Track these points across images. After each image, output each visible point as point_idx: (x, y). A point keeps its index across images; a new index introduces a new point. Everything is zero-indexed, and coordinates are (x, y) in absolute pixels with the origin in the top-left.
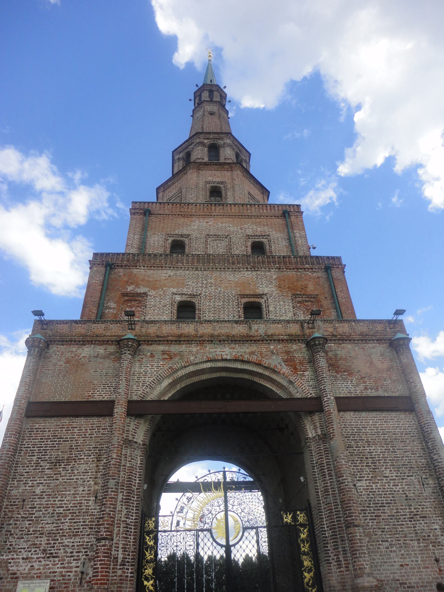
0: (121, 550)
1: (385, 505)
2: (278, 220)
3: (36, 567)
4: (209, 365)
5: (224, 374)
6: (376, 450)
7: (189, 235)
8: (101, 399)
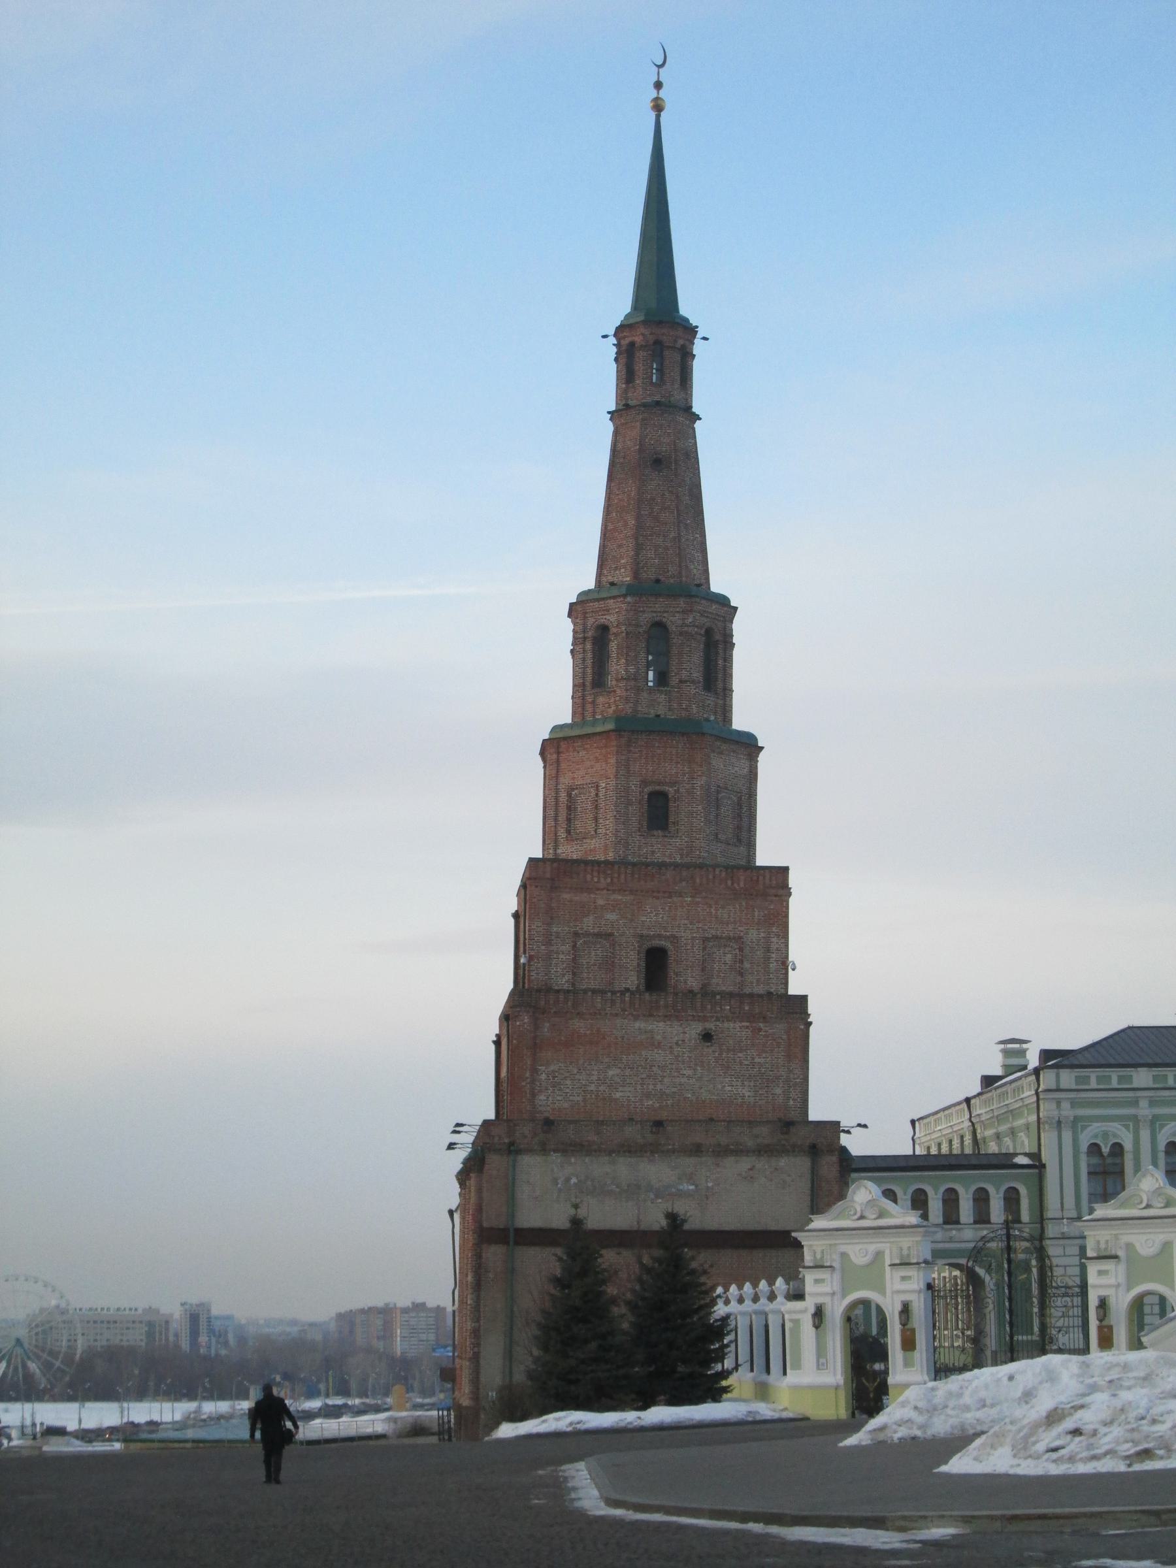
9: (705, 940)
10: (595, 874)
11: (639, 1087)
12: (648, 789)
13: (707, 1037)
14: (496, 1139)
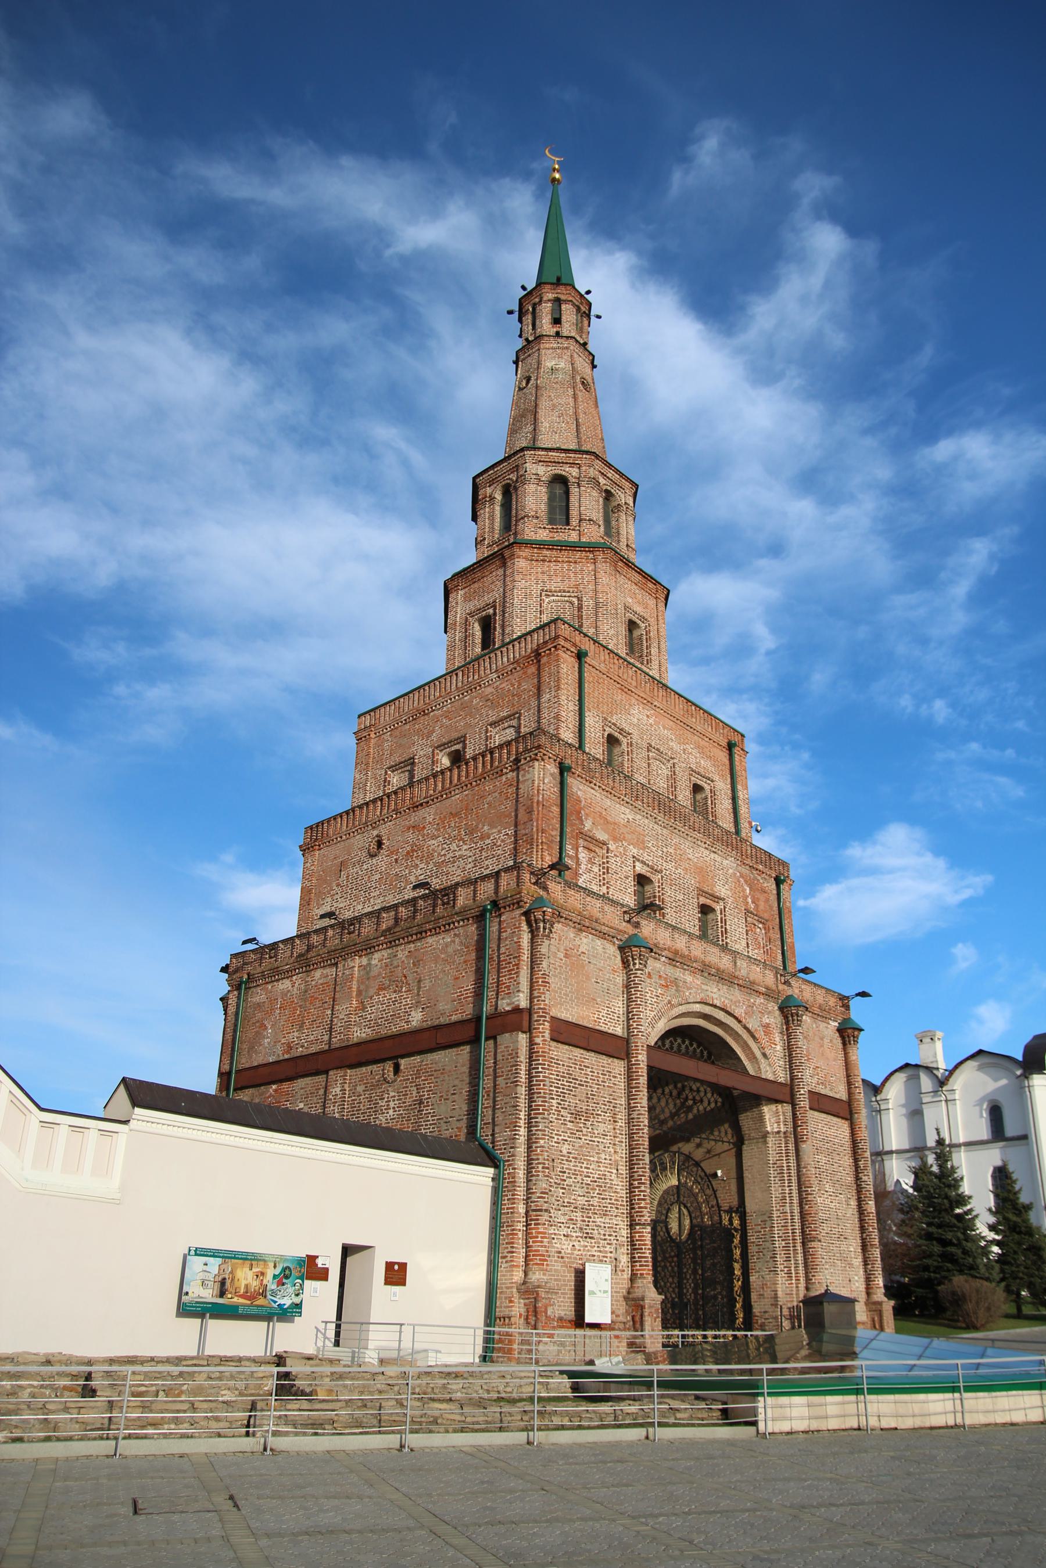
2: (721, 753)
3: (577, 1248)
4: (697, 1008)
6: (822, 1159)
7: (629, 734)
8: (606, 1030)
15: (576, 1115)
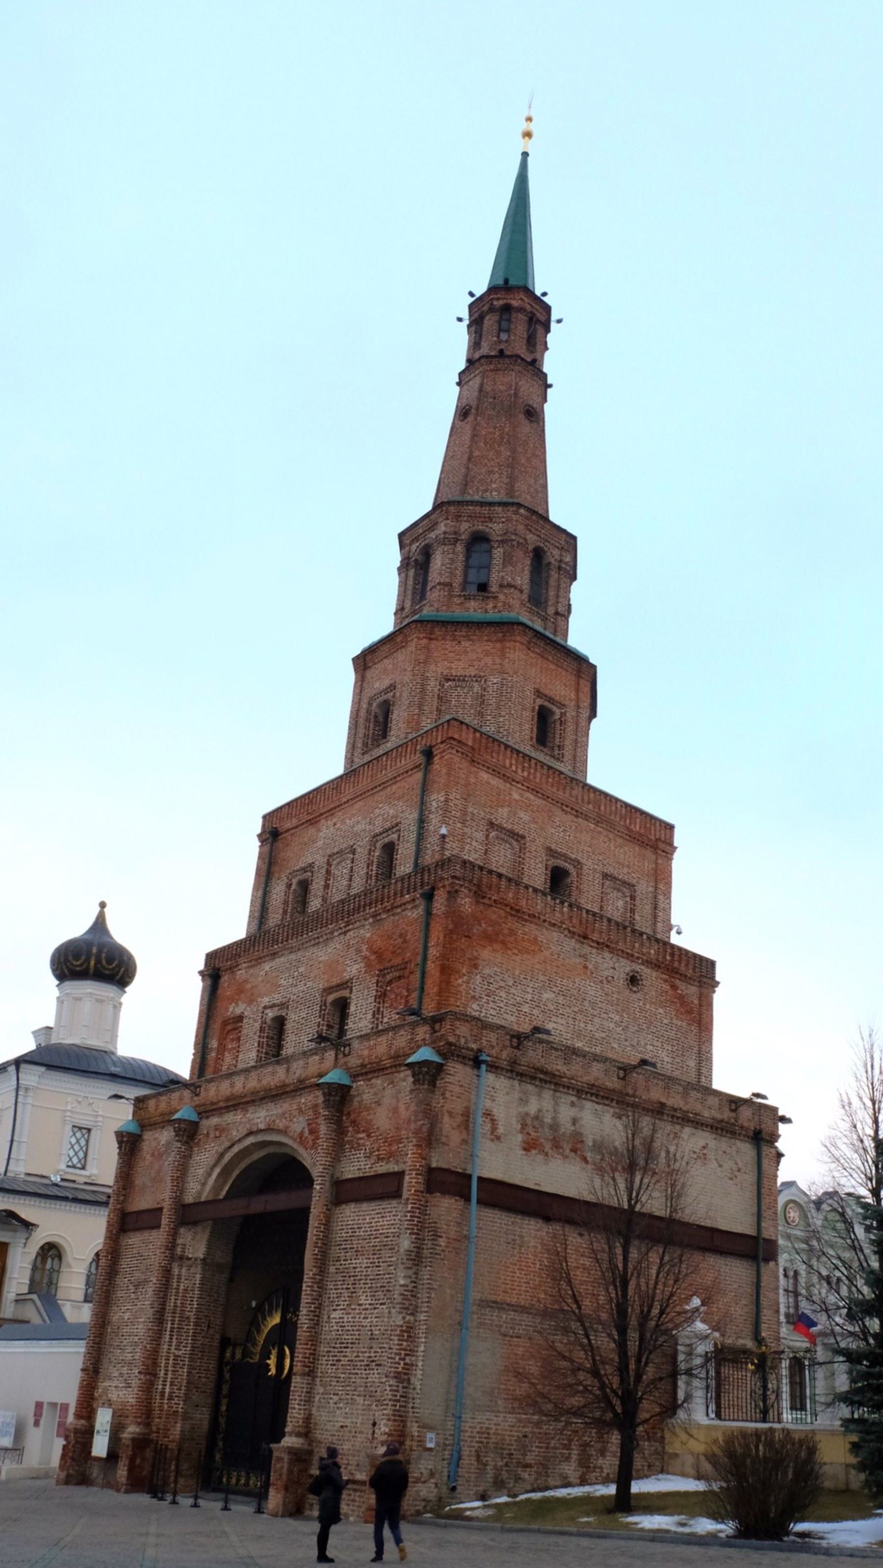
0: (168, 1383)
1: (349, 1345)
4: (251, 1140)
5: (271, 1150)
9: (605, 876)
10: (514, 762)
11: (571, 1021)
12: (539, 702)
13: (633, 980)
14: (463, 1041)
15: (137, 1286)
